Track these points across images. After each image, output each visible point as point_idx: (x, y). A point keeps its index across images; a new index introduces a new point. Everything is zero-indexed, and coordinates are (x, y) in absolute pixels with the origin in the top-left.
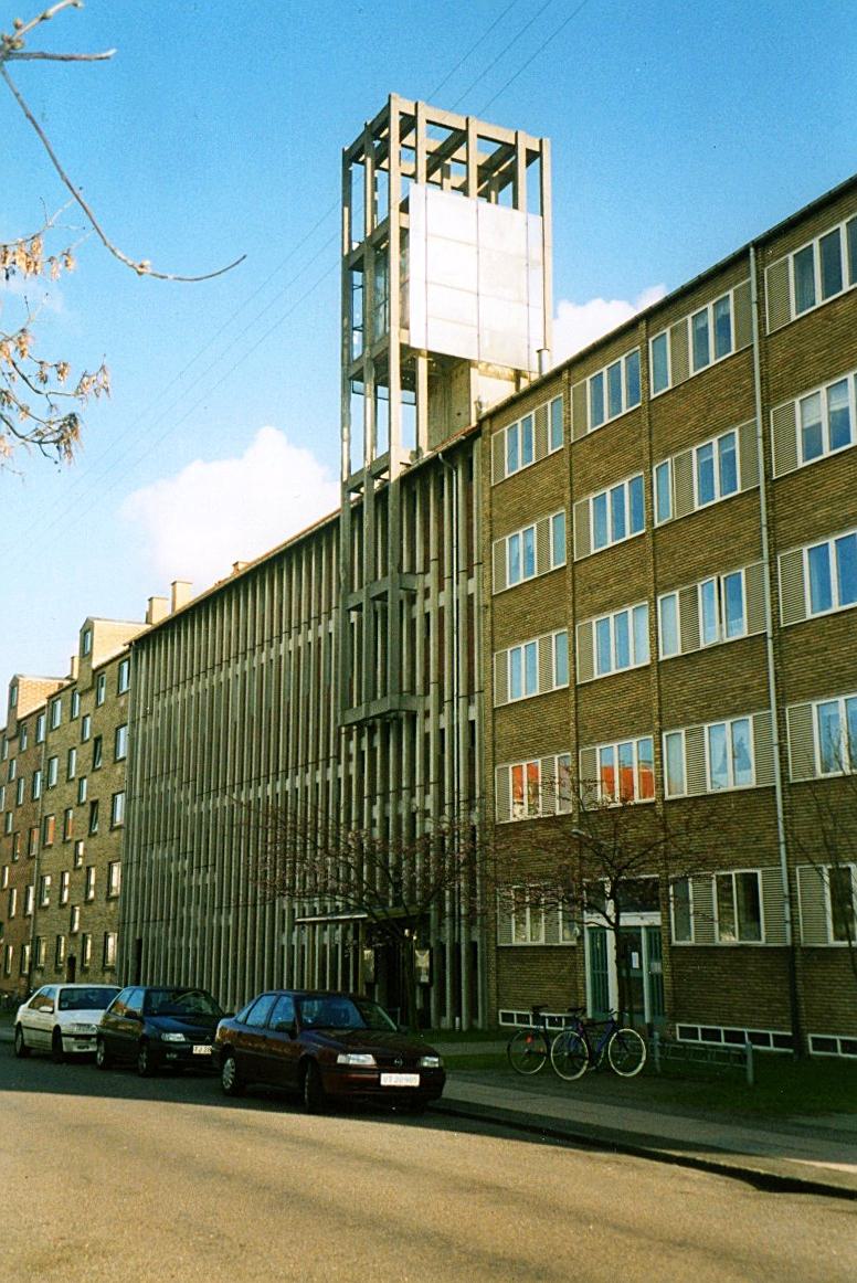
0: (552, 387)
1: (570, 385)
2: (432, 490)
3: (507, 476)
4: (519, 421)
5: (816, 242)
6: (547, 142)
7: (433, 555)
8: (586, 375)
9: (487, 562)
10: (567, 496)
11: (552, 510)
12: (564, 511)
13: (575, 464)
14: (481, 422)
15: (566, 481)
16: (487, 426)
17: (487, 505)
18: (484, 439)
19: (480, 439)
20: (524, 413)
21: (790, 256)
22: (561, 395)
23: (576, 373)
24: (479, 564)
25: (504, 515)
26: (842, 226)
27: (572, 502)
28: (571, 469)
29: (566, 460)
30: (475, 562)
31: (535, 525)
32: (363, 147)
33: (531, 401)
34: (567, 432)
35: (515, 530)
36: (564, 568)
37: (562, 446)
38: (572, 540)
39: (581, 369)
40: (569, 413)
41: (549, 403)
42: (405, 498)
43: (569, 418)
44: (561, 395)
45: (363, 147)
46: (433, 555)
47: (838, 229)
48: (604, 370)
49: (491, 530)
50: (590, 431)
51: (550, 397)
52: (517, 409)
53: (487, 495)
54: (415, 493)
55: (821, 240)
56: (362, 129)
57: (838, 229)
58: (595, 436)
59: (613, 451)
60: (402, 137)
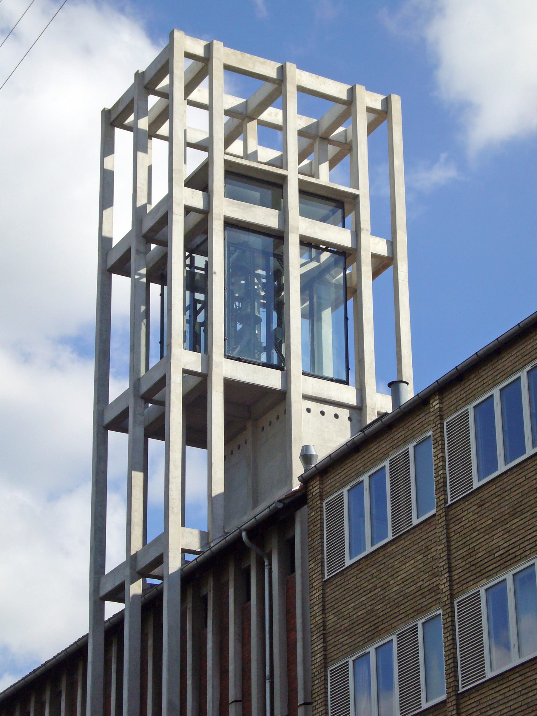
0: (415, 422)
1: (442, 418)
2: (231, 591)
3: (348, 562)
4: (365, 478)
5: (496, 392)
7: (233, 693)
8: (467, 402)
9: (319, 701)
10: (445, 587)
11: (421, 611)
12: (440, 611)
13: (454, 537)
14: (305, 480)
15: (442, 564)
16: (315, 488)
17: (317, 609)
18: (312, 509)
19: (305, 508)
20: (373, 465)
21: (470, 408)
22: (430, 433)
23: (451, 398)
24: (305, 704)
25: (346, 623)
26: (523, 375)
27: (452, 597)
28: (448, 546)
29: (440, 530)
30: (300, 701)
31: (394, 637)
33: (384, 444)
34: (441, 488)
35: (363, 646)
36: (444, 702)
37: (434, 512)
38: (455, 658)
39: (458, 392)
40: (443, 457)
41: (411, 447)
42: (190, 605)
43: (444, 468)
44: (430, 433)
46: (233, 693)
47: (519, 378)
48: (496, 392)
49: (325, 649)
50: (476, 484)
51: (413, 437)
52: (359, 460)
53: (317, 593)
54: (205, 598)
55: (501, 390)
57: (519, 378)
58: (485, 494)
59: (514, 513)
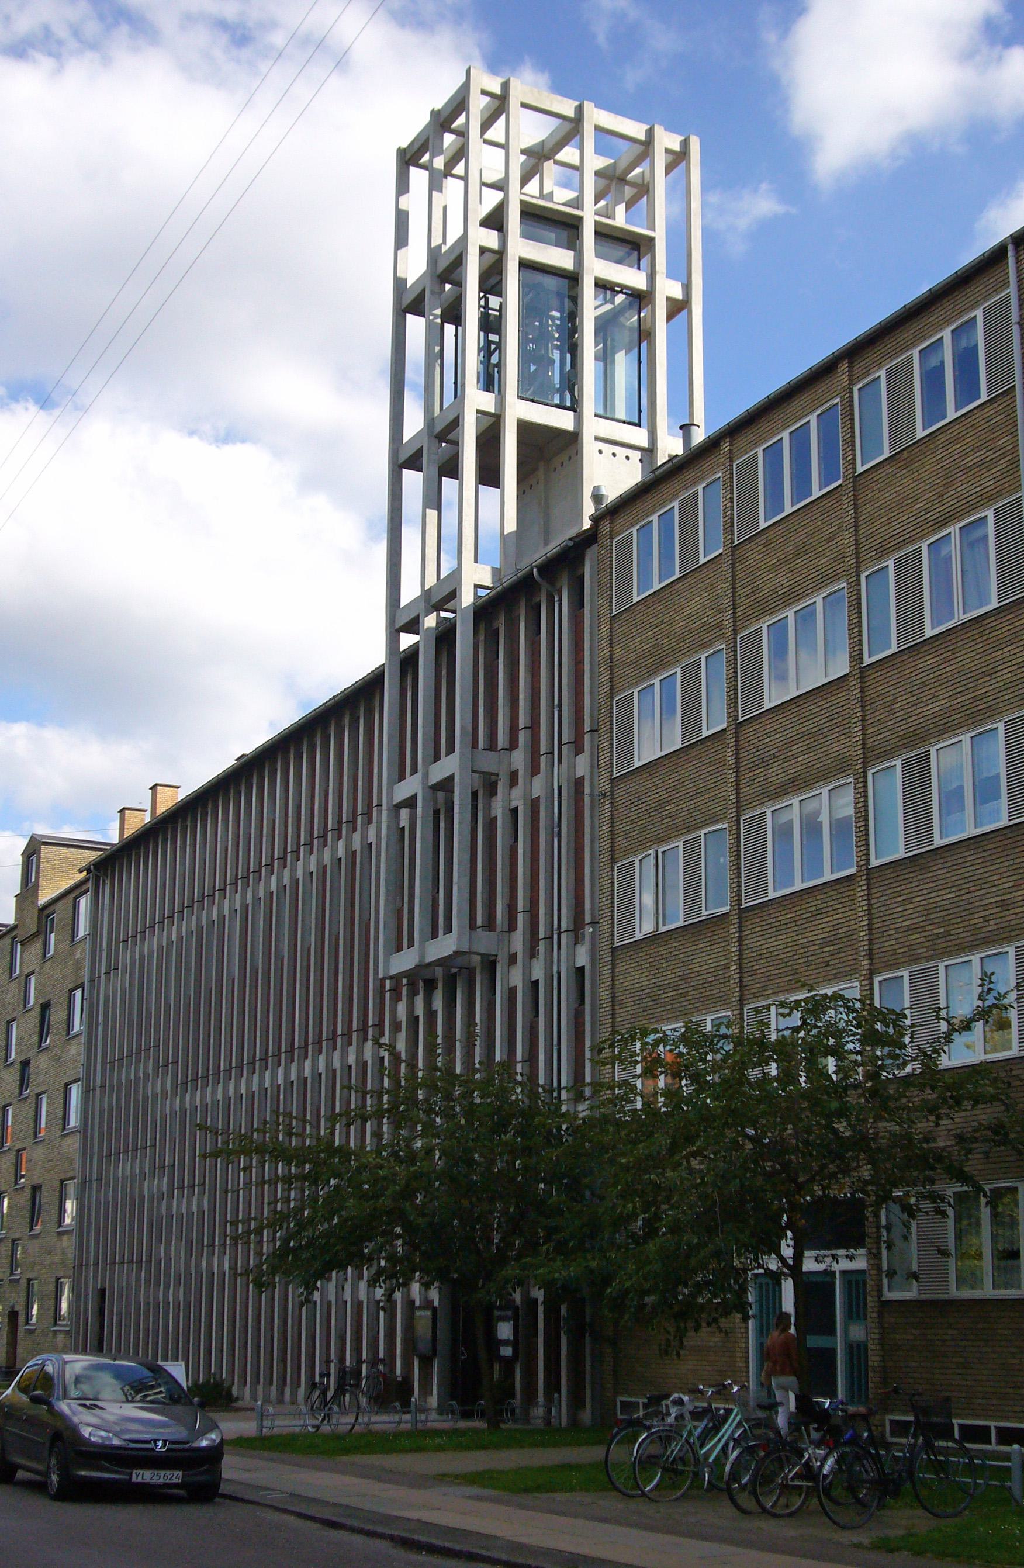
0: (705, 465)
1: (732, 461)
3: (636, 599)
4: (654, 518)
5: (785, 435)
6: (695, 144)
7: (523, 720)
8: (756, 444)
9: (604, 729)
10: (728, 623)
11: (704, 646)
12: (723, 646)
14: (596, 520)
16: (605, 527)
17: (604, 643)
19: (595, 547)
20: (662, 505)
21: (760, 451)
22: (719, 475)
23: (741, 441)
25: (632, 656)
27: (735, 632)
29: (726, 569)
30: (587, 728)
31: (678, 670)
32: (427, 141)
33: (675, 484)
34: (729, 528)
37: (721, 551)
39: (749, 435)
40: (732, 499)
41: (700, 488)
42: (482, 638)
44: (719, 475)
45: (427, 141)
46: (523, 720)
48: (785, 435)
49: (611, 680)
50: (763, 525)
51: (703, 479)
52: (649, 501)
53: (605, 628)
54: (497, 631)
55: (790, 433)
56: (426, 119)
58: (771, 534)
59: (798, 554)
60: (486, 126)
